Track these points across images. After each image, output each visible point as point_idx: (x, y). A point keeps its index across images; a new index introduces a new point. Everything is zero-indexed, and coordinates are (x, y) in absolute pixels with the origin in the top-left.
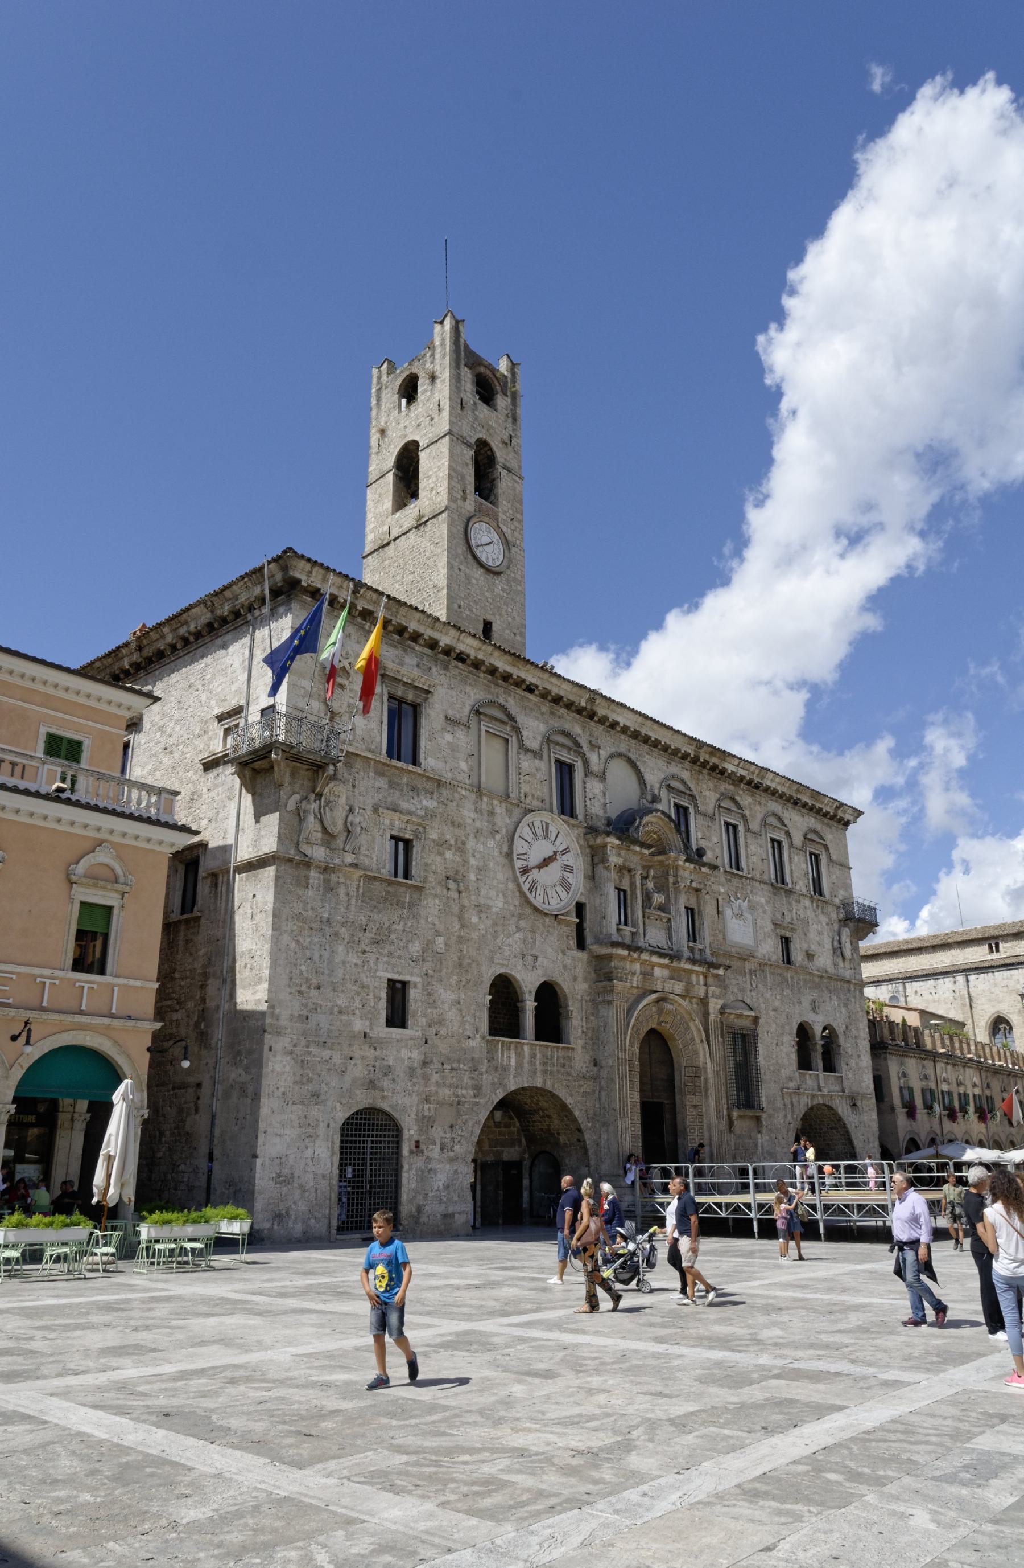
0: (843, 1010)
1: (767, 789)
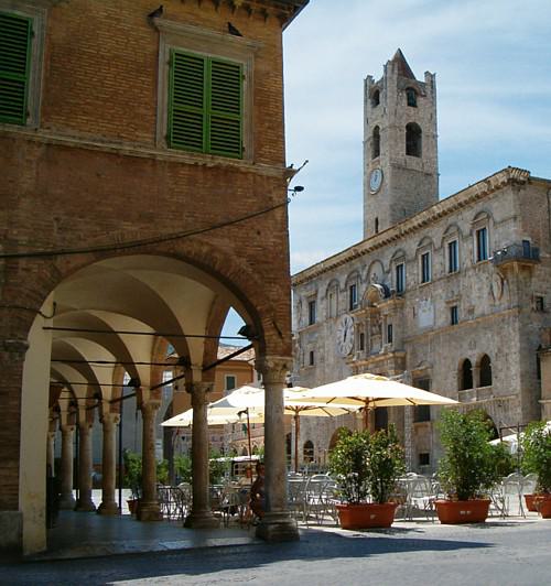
0: (496, 338)
1: (440, 216)
